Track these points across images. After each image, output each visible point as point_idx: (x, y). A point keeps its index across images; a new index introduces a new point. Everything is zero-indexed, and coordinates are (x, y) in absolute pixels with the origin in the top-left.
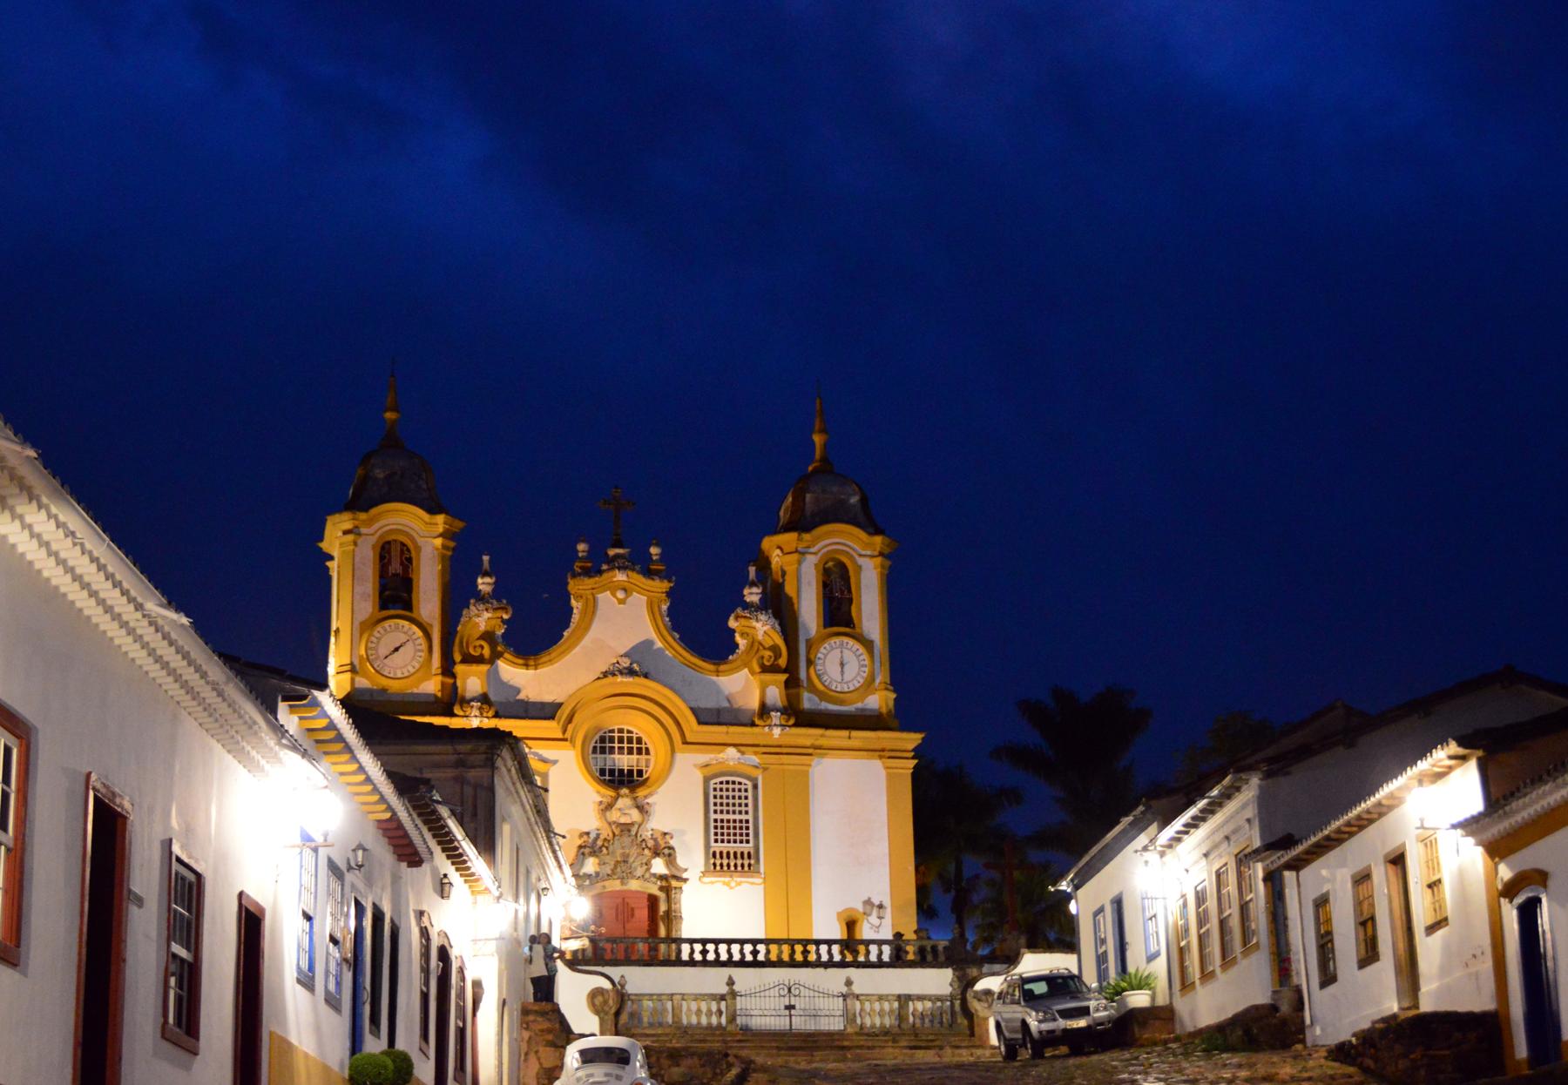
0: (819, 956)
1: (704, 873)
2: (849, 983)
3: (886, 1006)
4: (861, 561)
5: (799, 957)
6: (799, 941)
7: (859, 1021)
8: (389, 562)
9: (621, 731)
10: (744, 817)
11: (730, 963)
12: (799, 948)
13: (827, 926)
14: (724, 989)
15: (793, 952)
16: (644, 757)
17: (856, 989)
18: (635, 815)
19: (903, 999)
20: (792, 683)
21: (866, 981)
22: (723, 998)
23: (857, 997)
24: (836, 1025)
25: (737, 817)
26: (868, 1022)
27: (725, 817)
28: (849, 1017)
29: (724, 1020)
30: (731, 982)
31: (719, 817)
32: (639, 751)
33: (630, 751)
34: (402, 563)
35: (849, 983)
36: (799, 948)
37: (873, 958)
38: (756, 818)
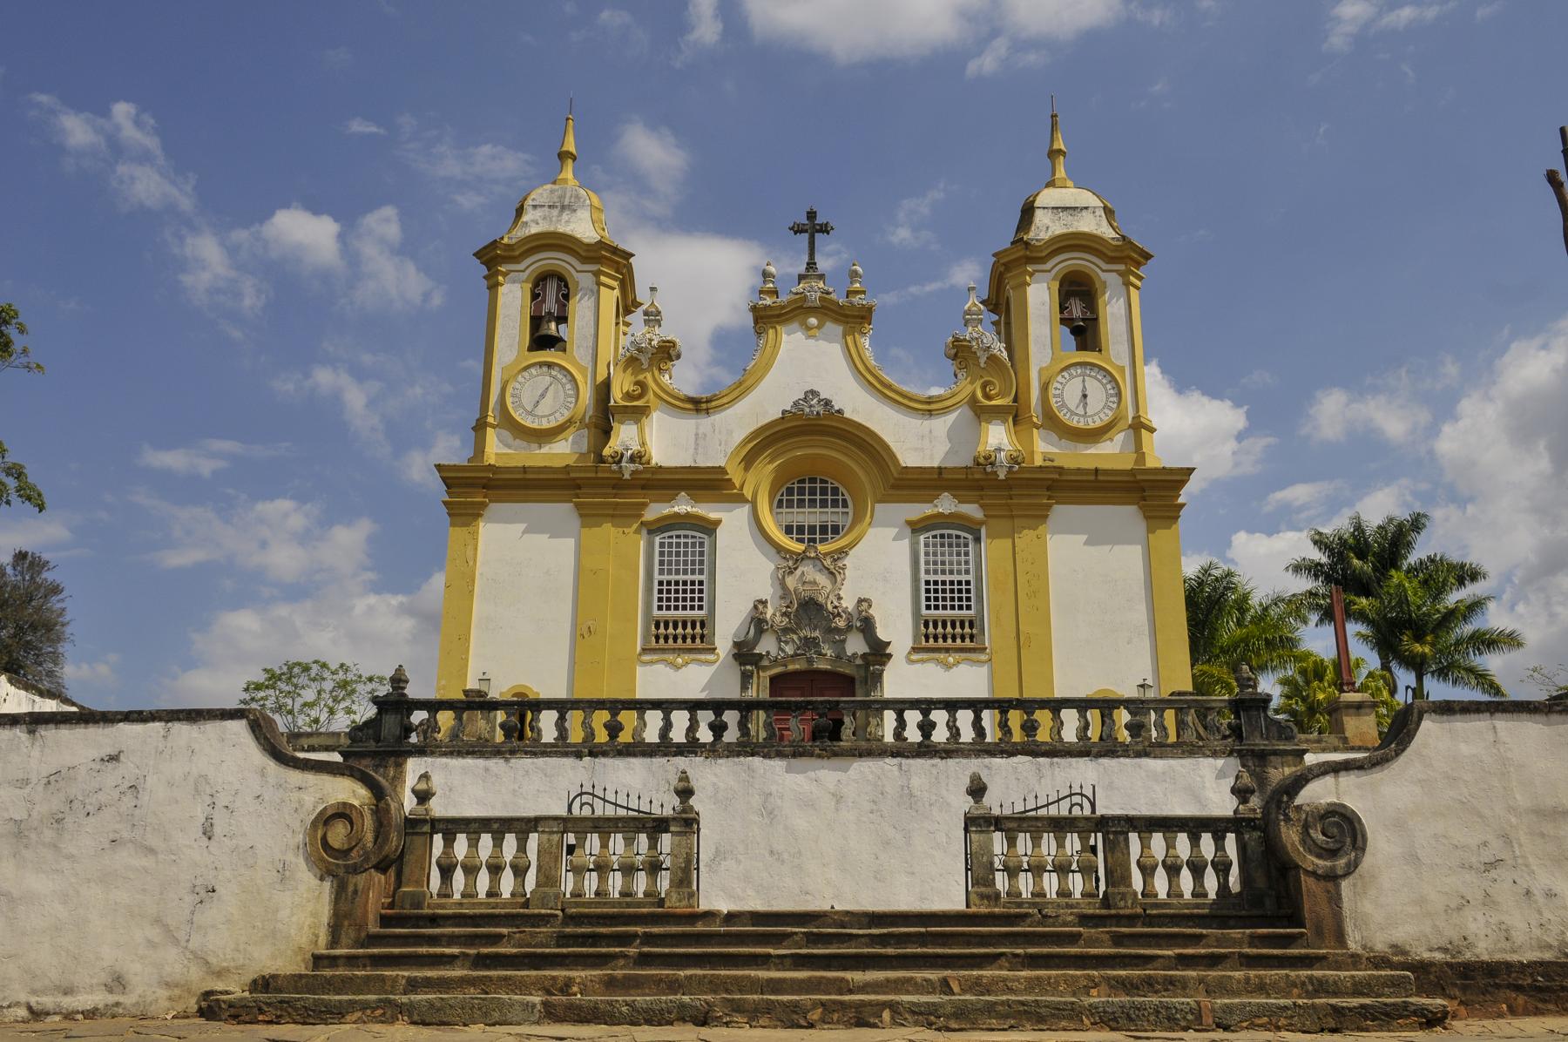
0: (955, 732)
1: (915, 650)
2: (977, 790)
3: (1073, 843)
4: (1103, 276)
5: (913, 735)
6: (914, 704)
7: (1001, 882)
8: (544, 301)
9: (812, 480)
10: (964, 578)
12: (912, 717)
14: (667, 805)
15: (901, 724)
16: (840, 510)
17: (995, 802)
18: (823, 580)
19: (1115, 828)
21: (1016, 784)
22: (657, 826)
23: (997, 823)
24: (947, 892)
25: (955, 578)
26: (1025, 884)
27: (940, 578)
28: (978, 871)
29: (664, 882)
30: (685, 793)
31: (932, 578)
32: (835, 503)
33: (824, 504)
34: (557, 301)
35: (977, 790)
36: (912, 717)
37: (1070, 735)
38: (979, 579)
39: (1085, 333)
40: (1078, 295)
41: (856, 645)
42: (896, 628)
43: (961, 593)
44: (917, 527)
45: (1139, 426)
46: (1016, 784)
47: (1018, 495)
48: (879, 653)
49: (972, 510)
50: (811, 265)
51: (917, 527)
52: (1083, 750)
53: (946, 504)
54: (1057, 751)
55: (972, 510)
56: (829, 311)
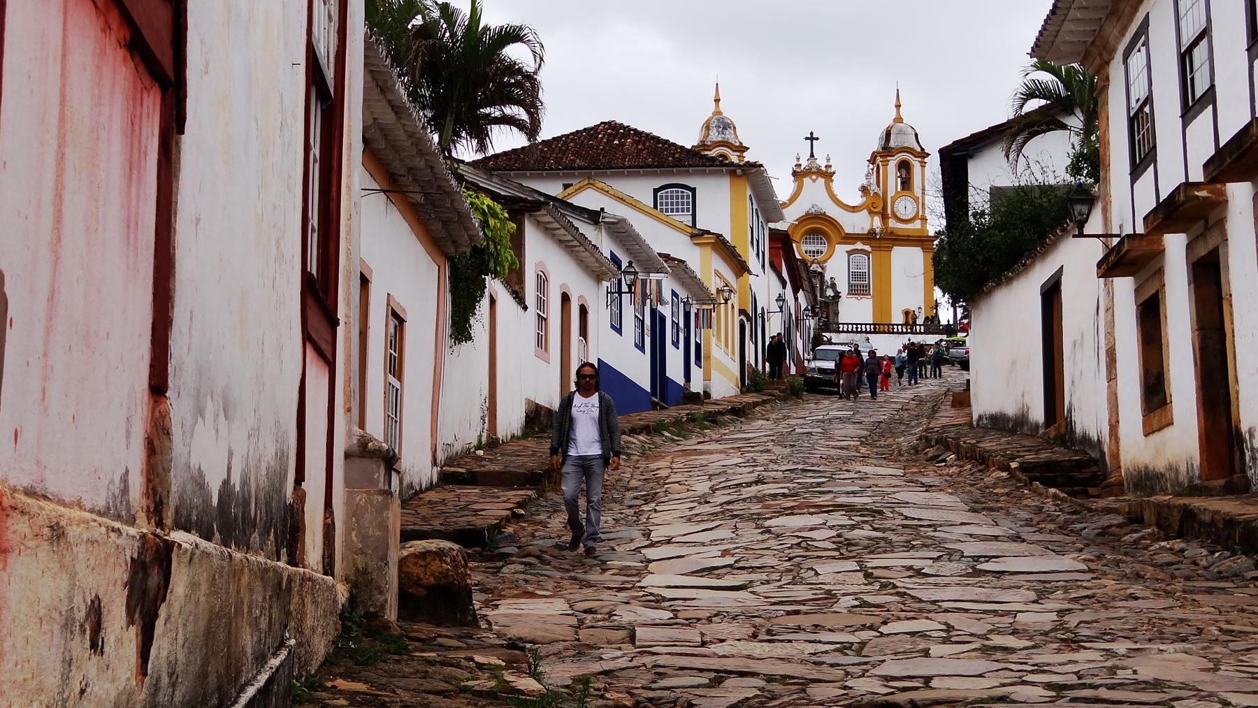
11: (866, 332)
13: (898, 318)
20: (884, 217)
39: (906, 184)
40: (904, 166)
41: (830, 293)
42: (843, 288)
43: (861, 276)
44: (850, 253)
45: (924, 219)
46: (917, 339)
47: (882, 241)
48: (837, 296)
49: (868, 248)
50: (812, 155)
51: (850, 253)
52: (921, 333)
53: (859, 246)
54: (916, 333)
55: (868, 248)
56: (820, 173)
